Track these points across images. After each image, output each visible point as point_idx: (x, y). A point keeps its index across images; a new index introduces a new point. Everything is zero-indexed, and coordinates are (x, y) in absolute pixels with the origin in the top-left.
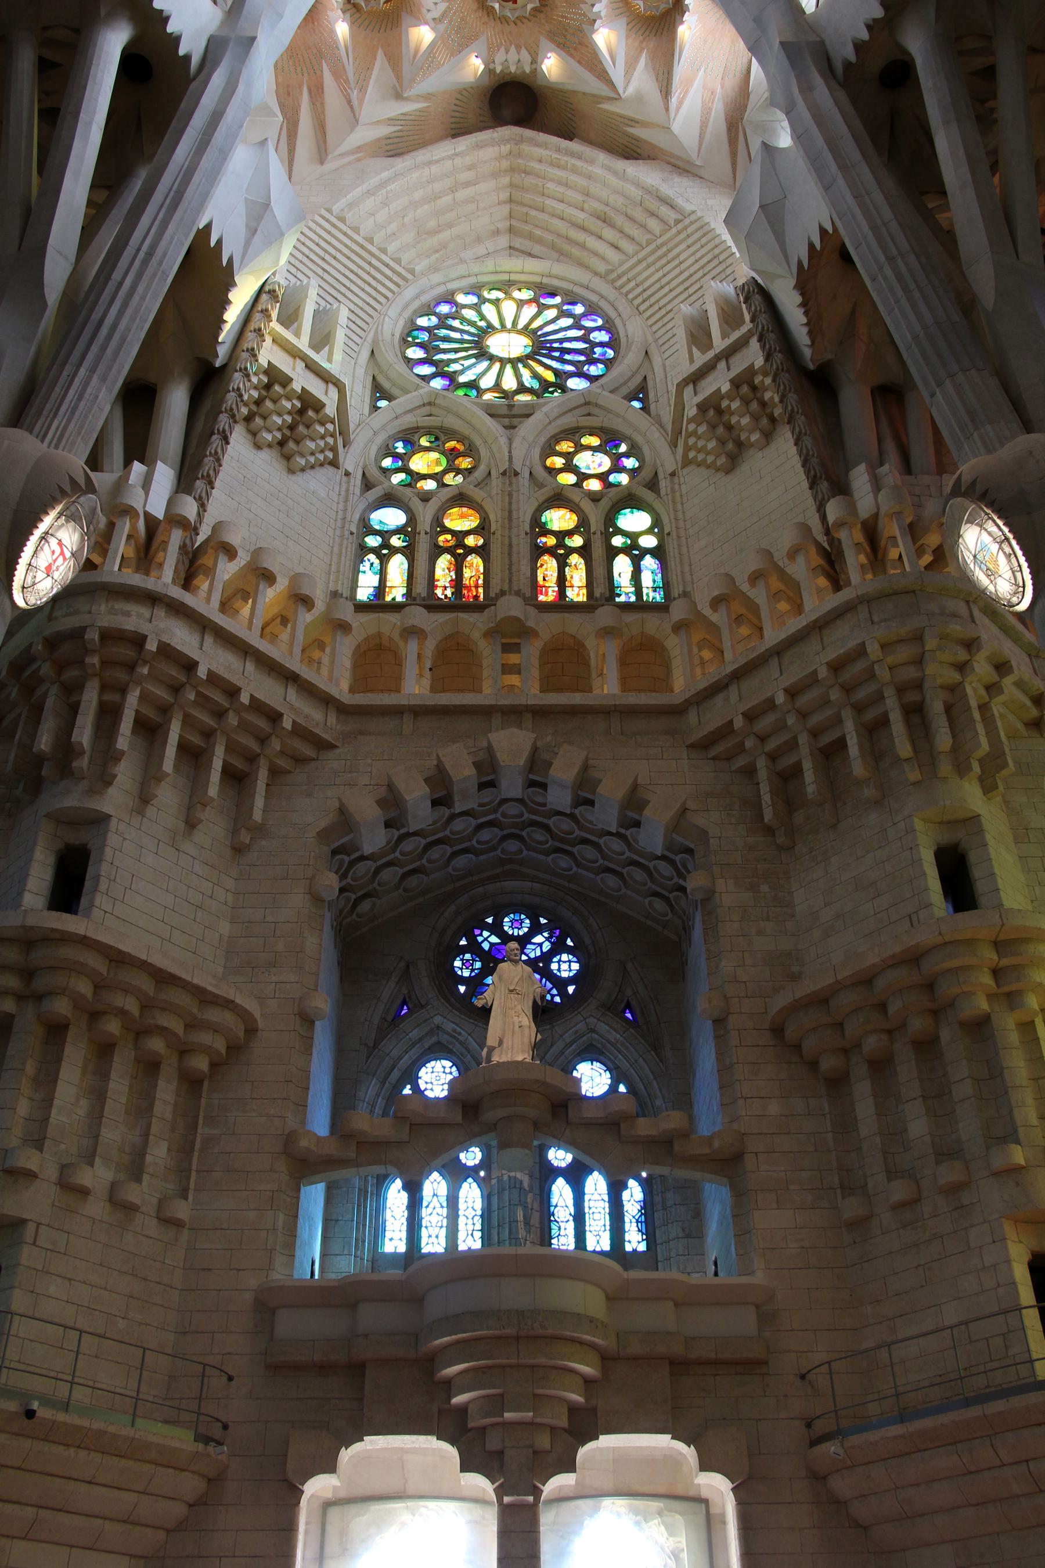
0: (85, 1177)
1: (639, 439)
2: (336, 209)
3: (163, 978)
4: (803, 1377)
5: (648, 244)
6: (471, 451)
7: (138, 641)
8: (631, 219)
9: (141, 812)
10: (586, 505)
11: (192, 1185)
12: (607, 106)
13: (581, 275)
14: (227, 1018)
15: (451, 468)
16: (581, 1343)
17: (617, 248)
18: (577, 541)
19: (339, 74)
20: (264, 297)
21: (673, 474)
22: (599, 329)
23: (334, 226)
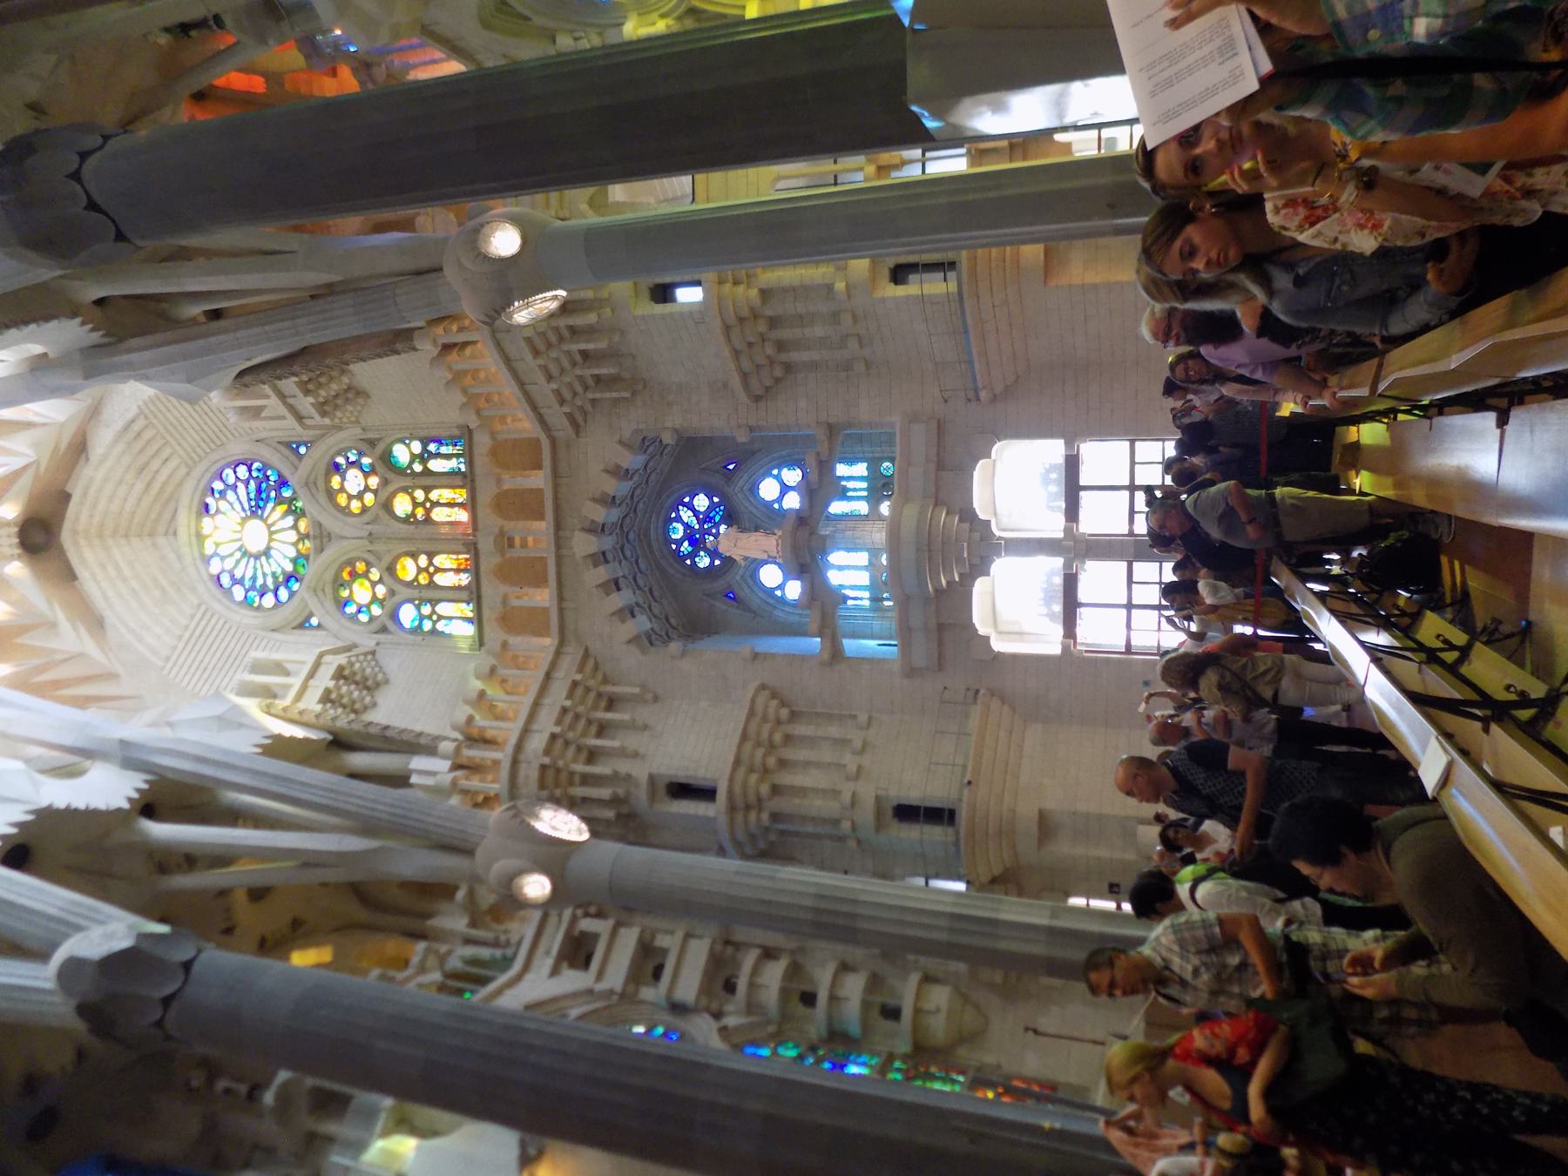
0: (852, 768)
1: (335, 449)
2: (160, 663)
3: (744, 737)
4: (946, 401)
5: (164, 438)
6: (351, 562)
7: (543, 768)
8: (141, 451)
9: (643, 757)
10: (391, 488)
11: (848, 713)
12: (42, 469)
13: (190, 485)
14: (760, 701)
15: (366, 575)
16: (931, 518)
17: (167, 460)
18: (420, 495)
19: (40, 669)
20: (272, 711)
21: (364, 430)
22: (235, 472)
23: (175, 664)
